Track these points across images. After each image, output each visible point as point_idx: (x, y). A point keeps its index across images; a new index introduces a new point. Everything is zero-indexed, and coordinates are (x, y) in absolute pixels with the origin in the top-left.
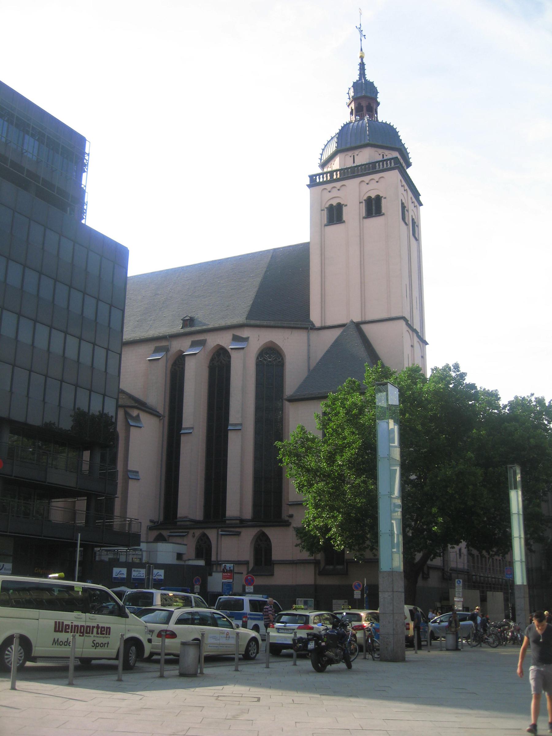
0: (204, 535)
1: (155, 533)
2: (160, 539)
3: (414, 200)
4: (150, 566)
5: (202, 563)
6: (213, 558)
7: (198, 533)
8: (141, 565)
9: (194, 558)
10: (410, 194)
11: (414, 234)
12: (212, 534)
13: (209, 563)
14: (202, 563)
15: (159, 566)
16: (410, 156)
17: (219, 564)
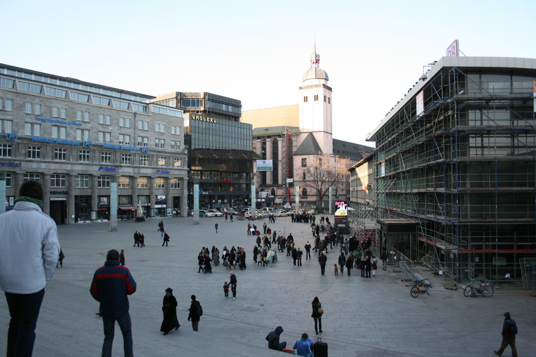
0: (273, 188)
1: (260, 188)
2: (262, 190)
3: (329, 91)
4: (261, 198)
5: (273, 197)
6: (276, 194)
7: (272, 188)
8: (259, 198)
9: (271, 194)
10: (328, 91)
11: (329, 103)
12: (275, 188)
13: (275, 195)
14: (273, 197)
15: (263, 198)
16: (329, 77)
17: (277, 196)
